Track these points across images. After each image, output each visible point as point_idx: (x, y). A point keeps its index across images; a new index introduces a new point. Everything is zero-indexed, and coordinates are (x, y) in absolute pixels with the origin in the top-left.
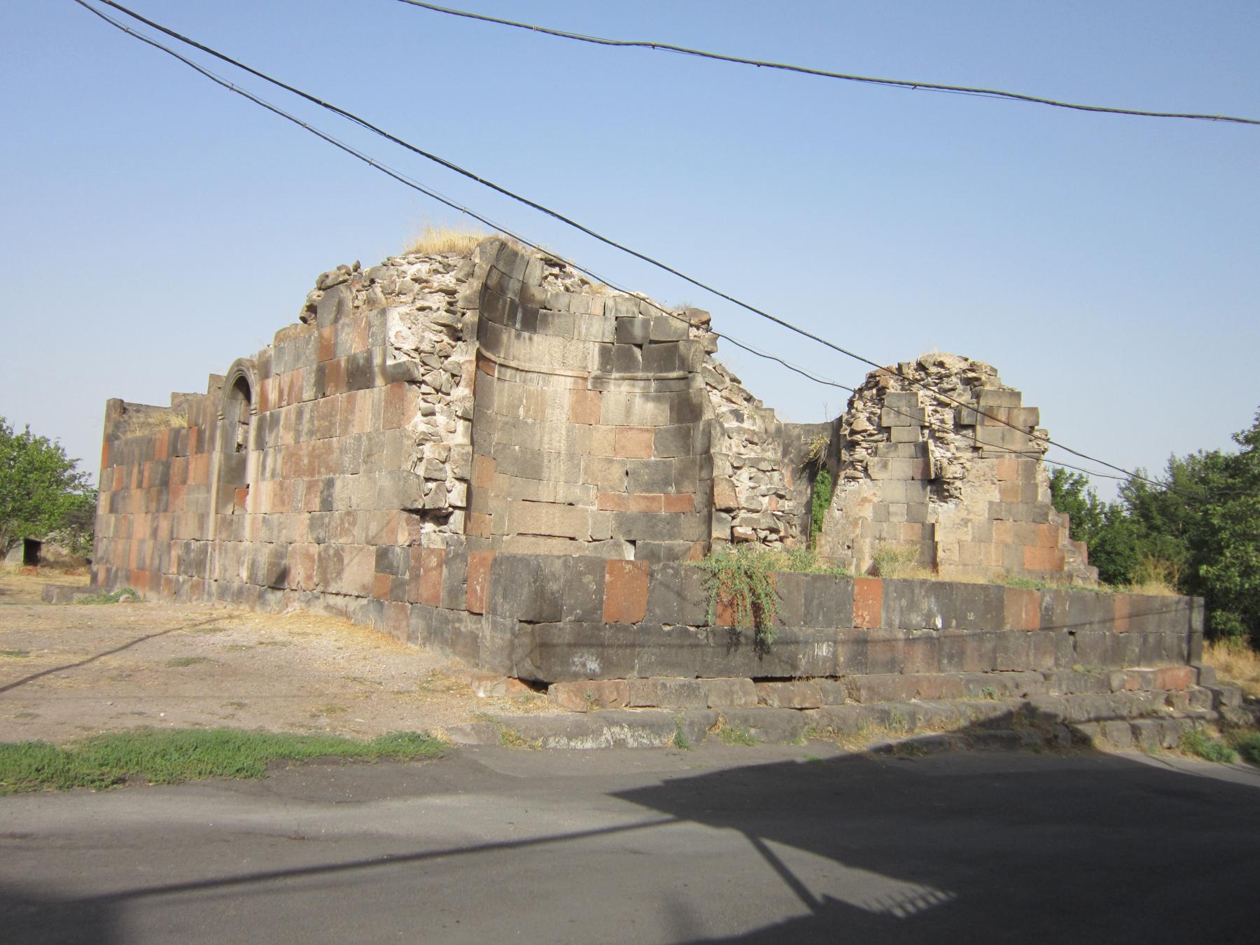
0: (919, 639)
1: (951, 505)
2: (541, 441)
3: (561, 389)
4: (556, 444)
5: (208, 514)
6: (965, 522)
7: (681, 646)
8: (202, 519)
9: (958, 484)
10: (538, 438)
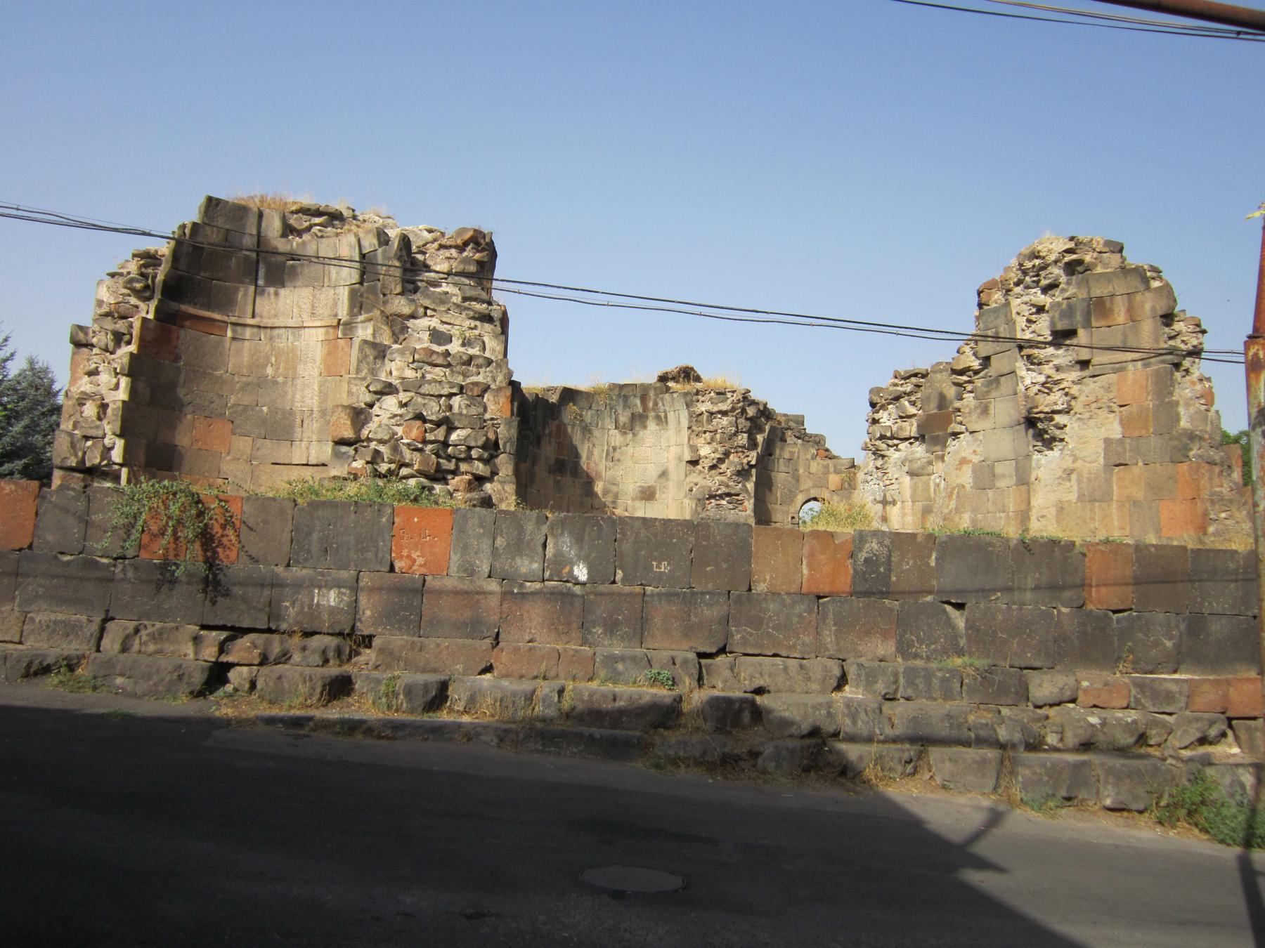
0: (532, 593)
1: (1054, 454)
2: (293, 401)
3: (313, 341)
4: (308, 401)
6: (1069, 473)
7: (82, 579)
9: (1059, 419)
10: (290, 397)
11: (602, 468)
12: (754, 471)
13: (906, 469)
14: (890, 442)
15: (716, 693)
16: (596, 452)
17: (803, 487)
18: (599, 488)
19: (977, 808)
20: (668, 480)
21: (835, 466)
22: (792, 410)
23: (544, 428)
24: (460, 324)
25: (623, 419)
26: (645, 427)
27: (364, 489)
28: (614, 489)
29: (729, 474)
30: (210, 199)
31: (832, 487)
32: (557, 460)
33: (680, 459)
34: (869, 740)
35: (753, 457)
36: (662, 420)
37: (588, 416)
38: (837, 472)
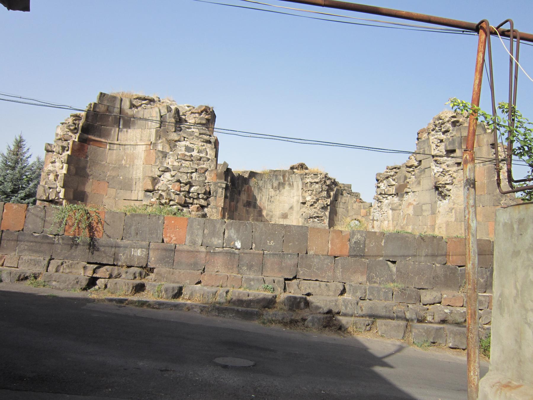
0: (218, 252)
1: (446, 202)
2: (132, 174)
3: (141, 150)
4: (138, 175)
6: (451, 209)
7: (42, 243)
9: (447, 186)
10: (131, 173)
11: (266, 205)
12: (329, 207)
13: (390, 207)
14: (384, 196)
15: (291, 295)
16: (264, 198)
17: (350, 214)
18: (264, 213)
19: (394, 345)
20: (293, 210)
21: (364, 206)
22: (346, 183)
23: (242, 188)
24: (198, 144)
25: (276, 184)
26: (284, 188)
27: (154, 210)
28: (271, 213)
29: (318, 208)
30: (101, 93)
31: (362, 215)
32: (247, 201)
33: (298, 201)
34: (352, 316)
35: (329, 201)
36: (291, 185)
37: (261, 183)
38: (364, 208)
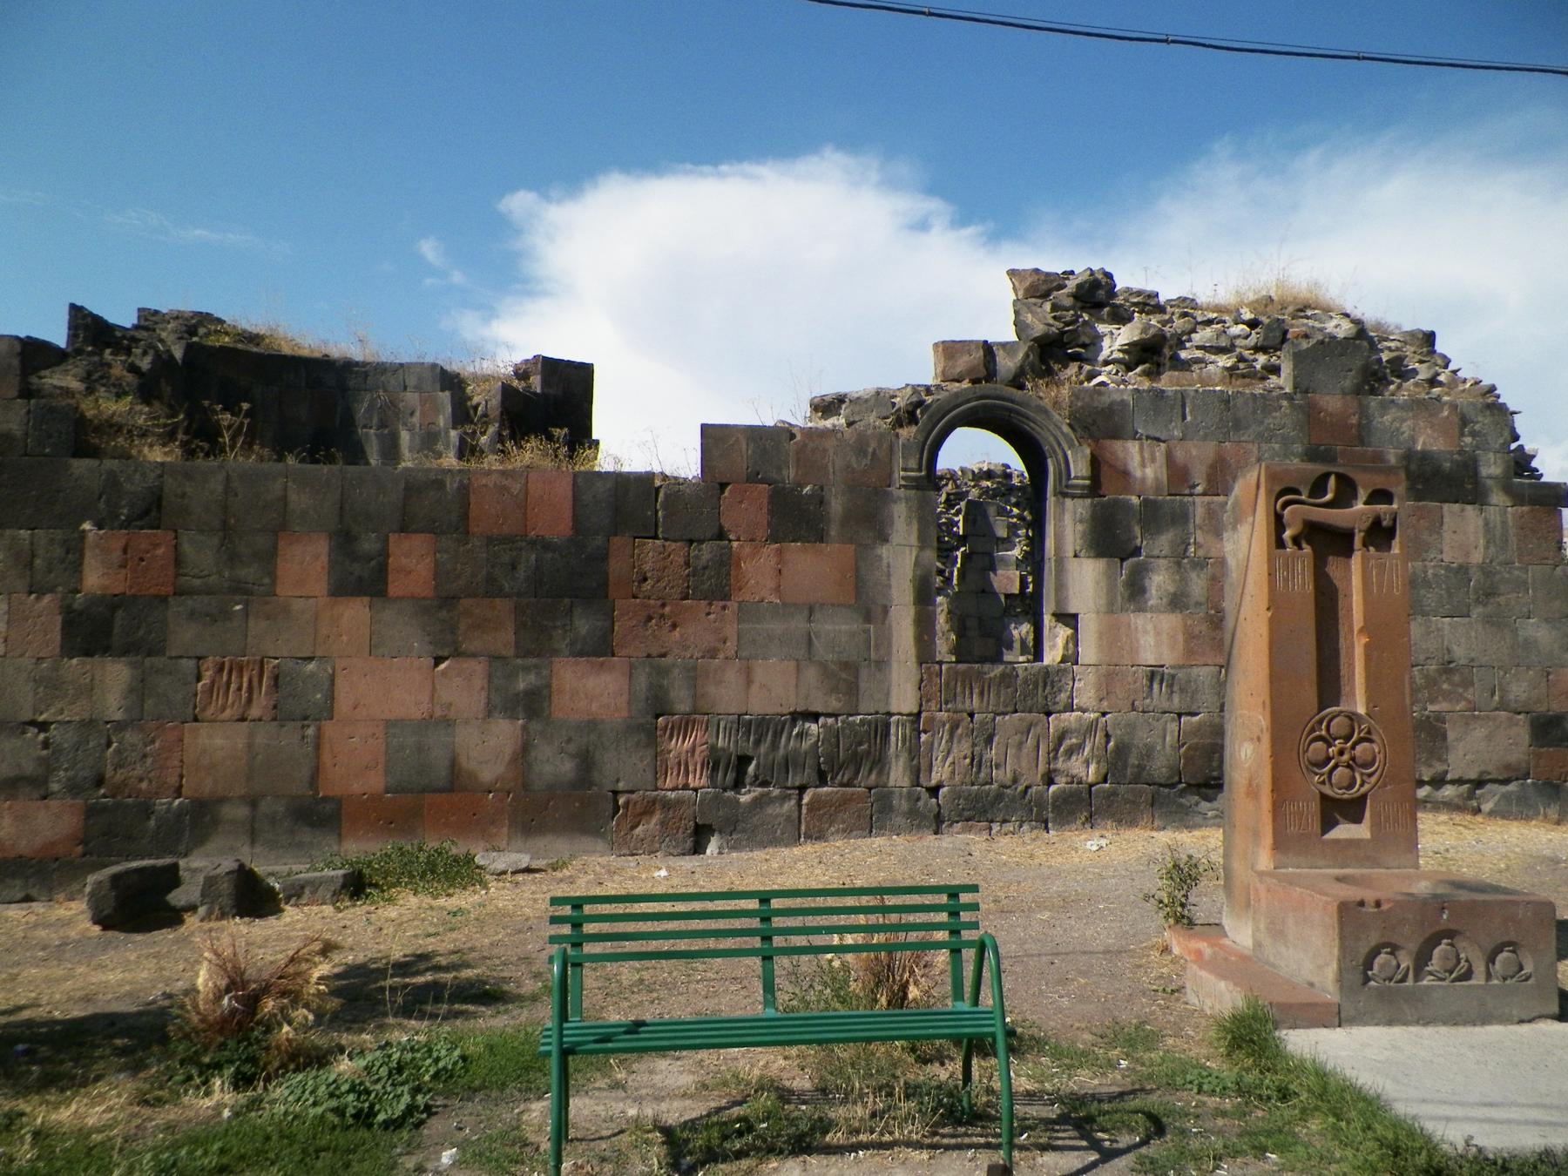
5: (882, 664)
8: (849, 676)
